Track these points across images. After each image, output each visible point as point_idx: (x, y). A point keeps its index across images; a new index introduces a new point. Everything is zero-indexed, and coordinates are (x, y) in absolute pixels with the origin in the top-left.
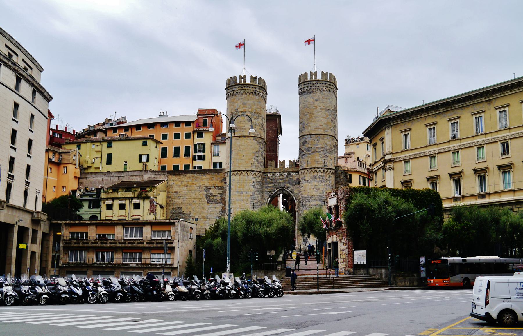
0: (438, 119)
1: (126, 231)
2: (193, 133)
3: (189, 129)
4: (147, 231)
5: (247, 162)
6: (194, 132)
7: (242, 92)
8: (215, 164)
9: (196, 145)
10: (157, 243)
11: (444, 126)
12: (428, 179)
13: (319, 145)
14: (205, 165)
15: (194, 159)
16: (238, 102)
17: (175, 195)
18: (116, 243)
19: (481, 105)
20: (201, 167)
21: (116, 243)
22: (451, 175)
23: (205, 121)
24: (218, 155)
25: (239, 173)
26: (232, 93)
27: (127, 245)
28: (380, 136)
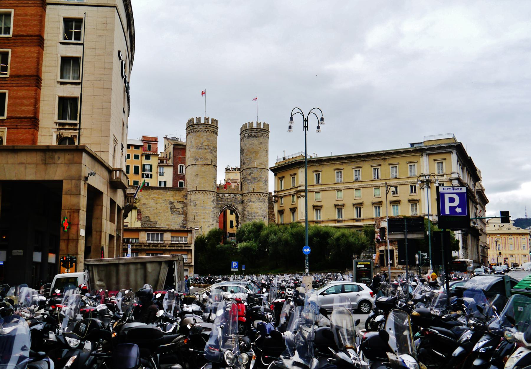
0: (344, 166)
1: (148, 237)
2: (142, 155)
3: (139, 152)
4: (168, 237)
5: (209, 185)
6: (142, 155)
7: (207, 130)
8: (160, 182)
9: (144, 165)
10: (177, 246)
11: (348, 172)
12: (336, 206)
13: (263, 177)
14: (153, 182)
15: (143, 176)
16: (204, 137)
17: (143, 206)
18: (141, 246)
19: (378, 161)
20: (148, 184)
21: (141, 246)
22: (354, 205)
23: (149, 146)
24: (163, 175)
25: (204, 192)
26: (198, 130)
27: (151, 248)
28: (292, 172)
